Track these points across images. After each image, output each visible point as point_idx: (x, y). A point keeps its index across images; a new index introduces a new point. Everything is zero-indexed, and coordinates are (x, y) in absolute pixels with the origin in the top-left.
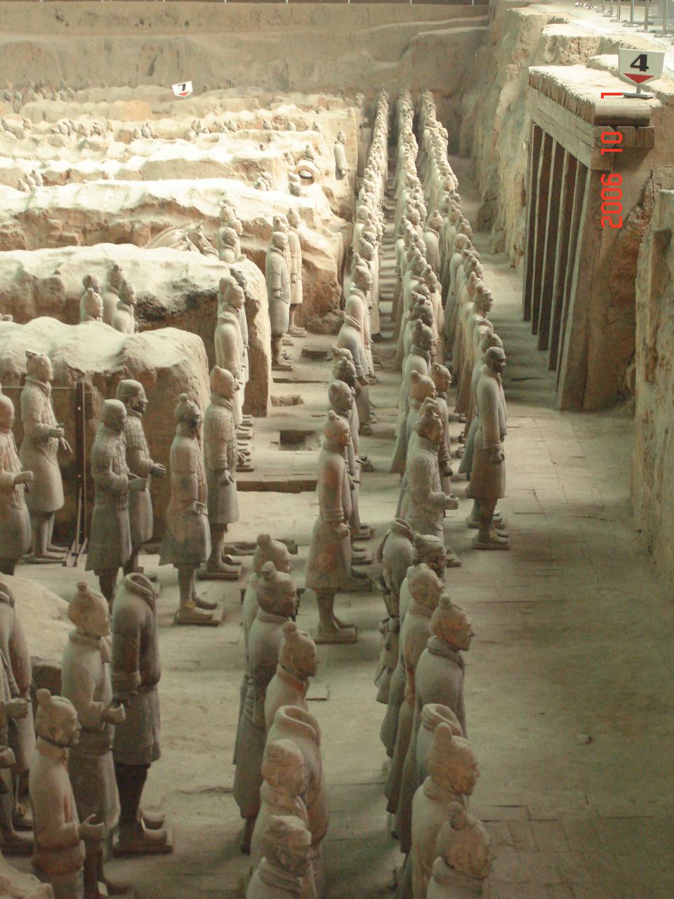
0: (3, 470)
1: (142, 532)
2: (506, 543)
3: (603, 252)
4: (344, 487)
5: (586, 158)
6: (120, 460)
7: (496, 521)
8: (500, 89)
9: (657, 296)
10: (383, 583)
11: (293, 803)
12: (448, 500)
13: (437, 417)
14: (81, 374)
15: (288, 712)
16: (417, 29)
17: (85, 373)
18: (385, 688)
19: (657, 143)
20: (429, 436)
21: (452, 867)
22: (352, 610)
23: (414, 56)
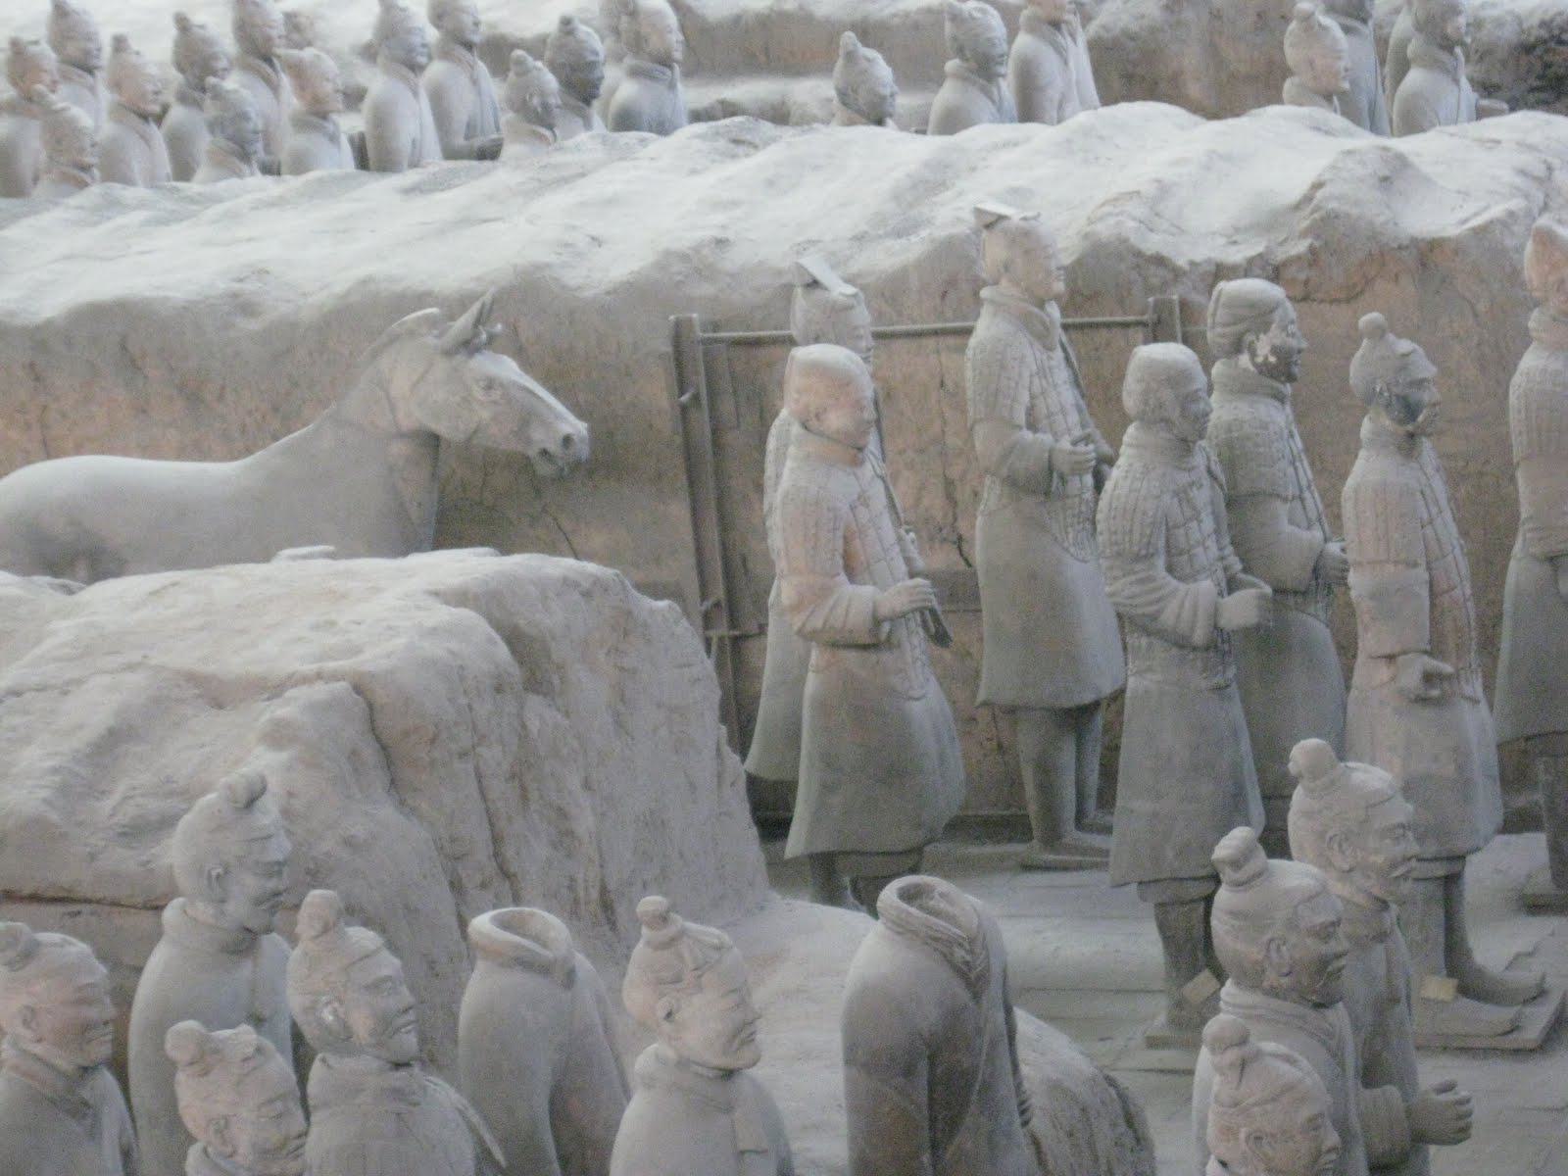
0: (843, 577)
6: (1196, 536)
14: (1177, 274)
17: (1187, 267)
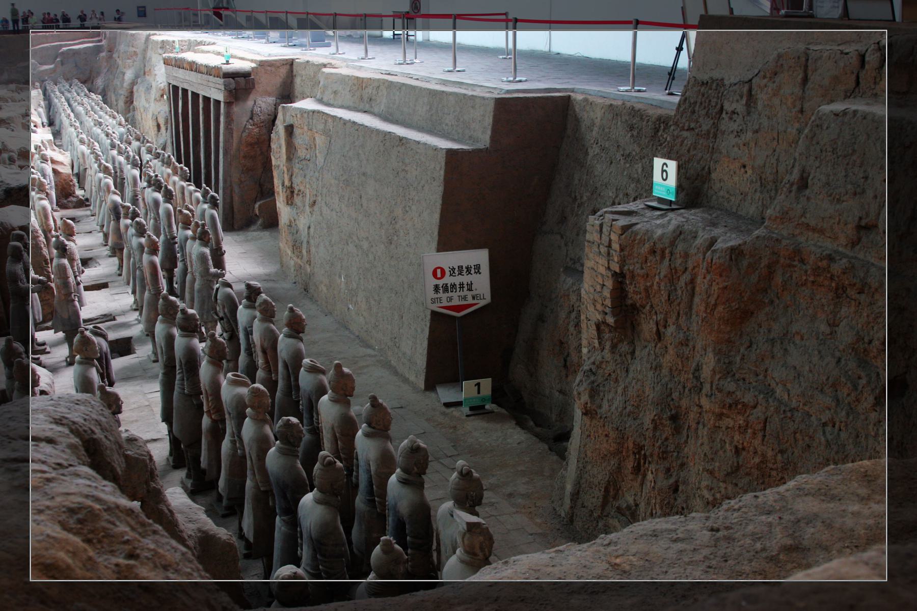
1: (37, 318)
3: (235, 144)
5: (220, 97)
8: (124, 74)
9: (289, 159)
16: (61, 46)
19: (256, 86)
21: (374, 428)
23: (62, 61)
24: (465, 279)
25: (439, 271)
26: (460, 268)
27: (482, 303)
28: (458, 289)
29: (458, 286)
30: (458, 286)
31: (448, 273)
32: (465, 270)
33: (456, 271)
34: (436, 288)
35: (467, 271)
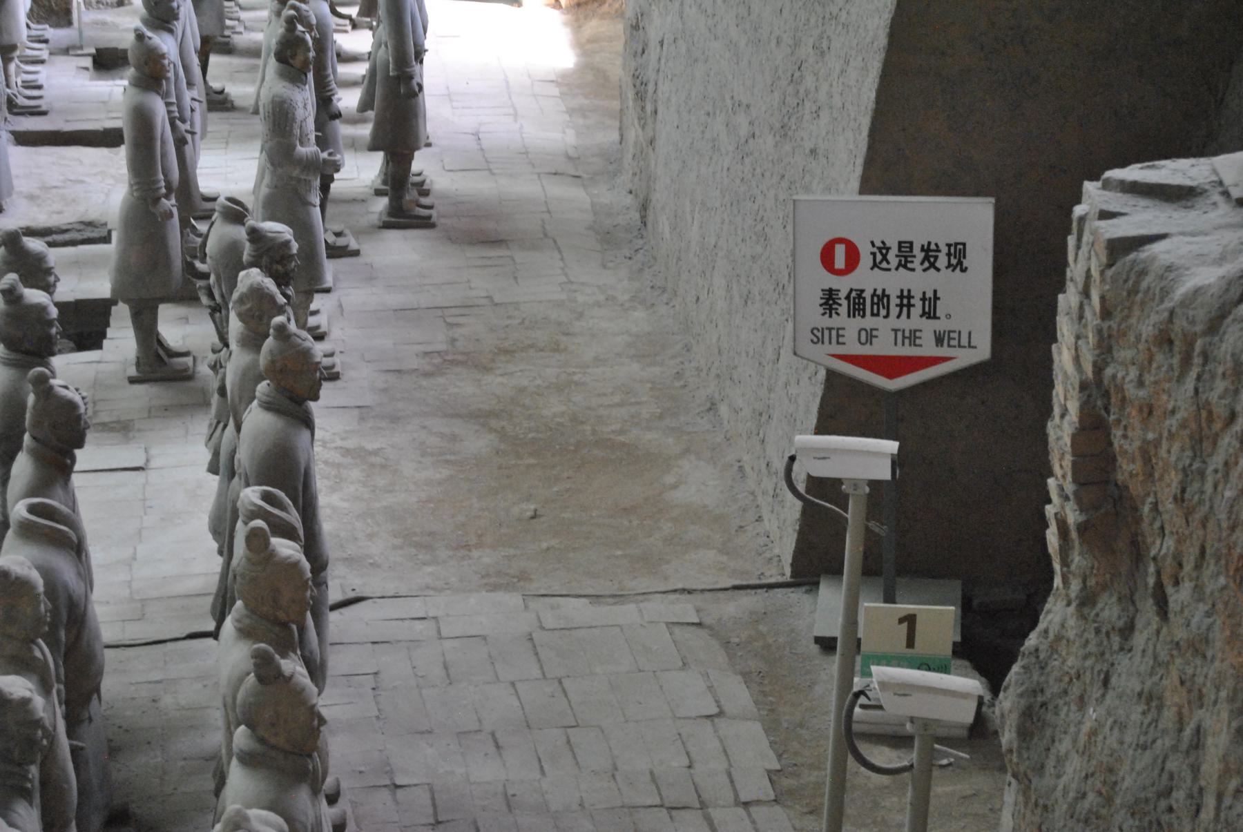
2: (430, 217)
4: (163, 142)
7: (414, 184)
10: (211, 295)
11: (30, 650)
12: (324, 160)
13: (304, 32)
15: (32, 509)
18: (216, 454)
20: (291, 61)
22: (189, 329)
24: (918, 281)
25: (840, 251)
26: (906, 248)
27: (963, 359)
28: (894, 310)
29: (894, 301)
30: (894, 301)
31: (866, 260)
32: (920, 256)
33: (892, 256)
34: (830, 300)
35: (926, 258)
